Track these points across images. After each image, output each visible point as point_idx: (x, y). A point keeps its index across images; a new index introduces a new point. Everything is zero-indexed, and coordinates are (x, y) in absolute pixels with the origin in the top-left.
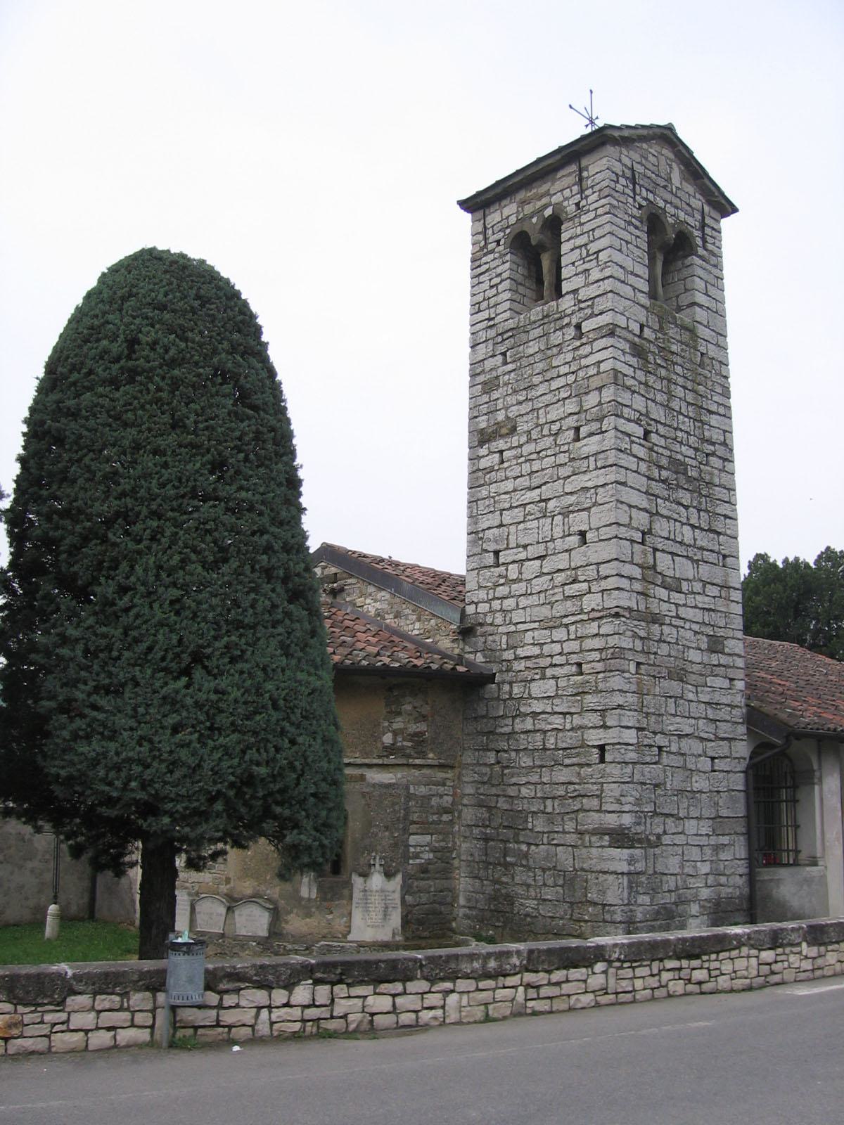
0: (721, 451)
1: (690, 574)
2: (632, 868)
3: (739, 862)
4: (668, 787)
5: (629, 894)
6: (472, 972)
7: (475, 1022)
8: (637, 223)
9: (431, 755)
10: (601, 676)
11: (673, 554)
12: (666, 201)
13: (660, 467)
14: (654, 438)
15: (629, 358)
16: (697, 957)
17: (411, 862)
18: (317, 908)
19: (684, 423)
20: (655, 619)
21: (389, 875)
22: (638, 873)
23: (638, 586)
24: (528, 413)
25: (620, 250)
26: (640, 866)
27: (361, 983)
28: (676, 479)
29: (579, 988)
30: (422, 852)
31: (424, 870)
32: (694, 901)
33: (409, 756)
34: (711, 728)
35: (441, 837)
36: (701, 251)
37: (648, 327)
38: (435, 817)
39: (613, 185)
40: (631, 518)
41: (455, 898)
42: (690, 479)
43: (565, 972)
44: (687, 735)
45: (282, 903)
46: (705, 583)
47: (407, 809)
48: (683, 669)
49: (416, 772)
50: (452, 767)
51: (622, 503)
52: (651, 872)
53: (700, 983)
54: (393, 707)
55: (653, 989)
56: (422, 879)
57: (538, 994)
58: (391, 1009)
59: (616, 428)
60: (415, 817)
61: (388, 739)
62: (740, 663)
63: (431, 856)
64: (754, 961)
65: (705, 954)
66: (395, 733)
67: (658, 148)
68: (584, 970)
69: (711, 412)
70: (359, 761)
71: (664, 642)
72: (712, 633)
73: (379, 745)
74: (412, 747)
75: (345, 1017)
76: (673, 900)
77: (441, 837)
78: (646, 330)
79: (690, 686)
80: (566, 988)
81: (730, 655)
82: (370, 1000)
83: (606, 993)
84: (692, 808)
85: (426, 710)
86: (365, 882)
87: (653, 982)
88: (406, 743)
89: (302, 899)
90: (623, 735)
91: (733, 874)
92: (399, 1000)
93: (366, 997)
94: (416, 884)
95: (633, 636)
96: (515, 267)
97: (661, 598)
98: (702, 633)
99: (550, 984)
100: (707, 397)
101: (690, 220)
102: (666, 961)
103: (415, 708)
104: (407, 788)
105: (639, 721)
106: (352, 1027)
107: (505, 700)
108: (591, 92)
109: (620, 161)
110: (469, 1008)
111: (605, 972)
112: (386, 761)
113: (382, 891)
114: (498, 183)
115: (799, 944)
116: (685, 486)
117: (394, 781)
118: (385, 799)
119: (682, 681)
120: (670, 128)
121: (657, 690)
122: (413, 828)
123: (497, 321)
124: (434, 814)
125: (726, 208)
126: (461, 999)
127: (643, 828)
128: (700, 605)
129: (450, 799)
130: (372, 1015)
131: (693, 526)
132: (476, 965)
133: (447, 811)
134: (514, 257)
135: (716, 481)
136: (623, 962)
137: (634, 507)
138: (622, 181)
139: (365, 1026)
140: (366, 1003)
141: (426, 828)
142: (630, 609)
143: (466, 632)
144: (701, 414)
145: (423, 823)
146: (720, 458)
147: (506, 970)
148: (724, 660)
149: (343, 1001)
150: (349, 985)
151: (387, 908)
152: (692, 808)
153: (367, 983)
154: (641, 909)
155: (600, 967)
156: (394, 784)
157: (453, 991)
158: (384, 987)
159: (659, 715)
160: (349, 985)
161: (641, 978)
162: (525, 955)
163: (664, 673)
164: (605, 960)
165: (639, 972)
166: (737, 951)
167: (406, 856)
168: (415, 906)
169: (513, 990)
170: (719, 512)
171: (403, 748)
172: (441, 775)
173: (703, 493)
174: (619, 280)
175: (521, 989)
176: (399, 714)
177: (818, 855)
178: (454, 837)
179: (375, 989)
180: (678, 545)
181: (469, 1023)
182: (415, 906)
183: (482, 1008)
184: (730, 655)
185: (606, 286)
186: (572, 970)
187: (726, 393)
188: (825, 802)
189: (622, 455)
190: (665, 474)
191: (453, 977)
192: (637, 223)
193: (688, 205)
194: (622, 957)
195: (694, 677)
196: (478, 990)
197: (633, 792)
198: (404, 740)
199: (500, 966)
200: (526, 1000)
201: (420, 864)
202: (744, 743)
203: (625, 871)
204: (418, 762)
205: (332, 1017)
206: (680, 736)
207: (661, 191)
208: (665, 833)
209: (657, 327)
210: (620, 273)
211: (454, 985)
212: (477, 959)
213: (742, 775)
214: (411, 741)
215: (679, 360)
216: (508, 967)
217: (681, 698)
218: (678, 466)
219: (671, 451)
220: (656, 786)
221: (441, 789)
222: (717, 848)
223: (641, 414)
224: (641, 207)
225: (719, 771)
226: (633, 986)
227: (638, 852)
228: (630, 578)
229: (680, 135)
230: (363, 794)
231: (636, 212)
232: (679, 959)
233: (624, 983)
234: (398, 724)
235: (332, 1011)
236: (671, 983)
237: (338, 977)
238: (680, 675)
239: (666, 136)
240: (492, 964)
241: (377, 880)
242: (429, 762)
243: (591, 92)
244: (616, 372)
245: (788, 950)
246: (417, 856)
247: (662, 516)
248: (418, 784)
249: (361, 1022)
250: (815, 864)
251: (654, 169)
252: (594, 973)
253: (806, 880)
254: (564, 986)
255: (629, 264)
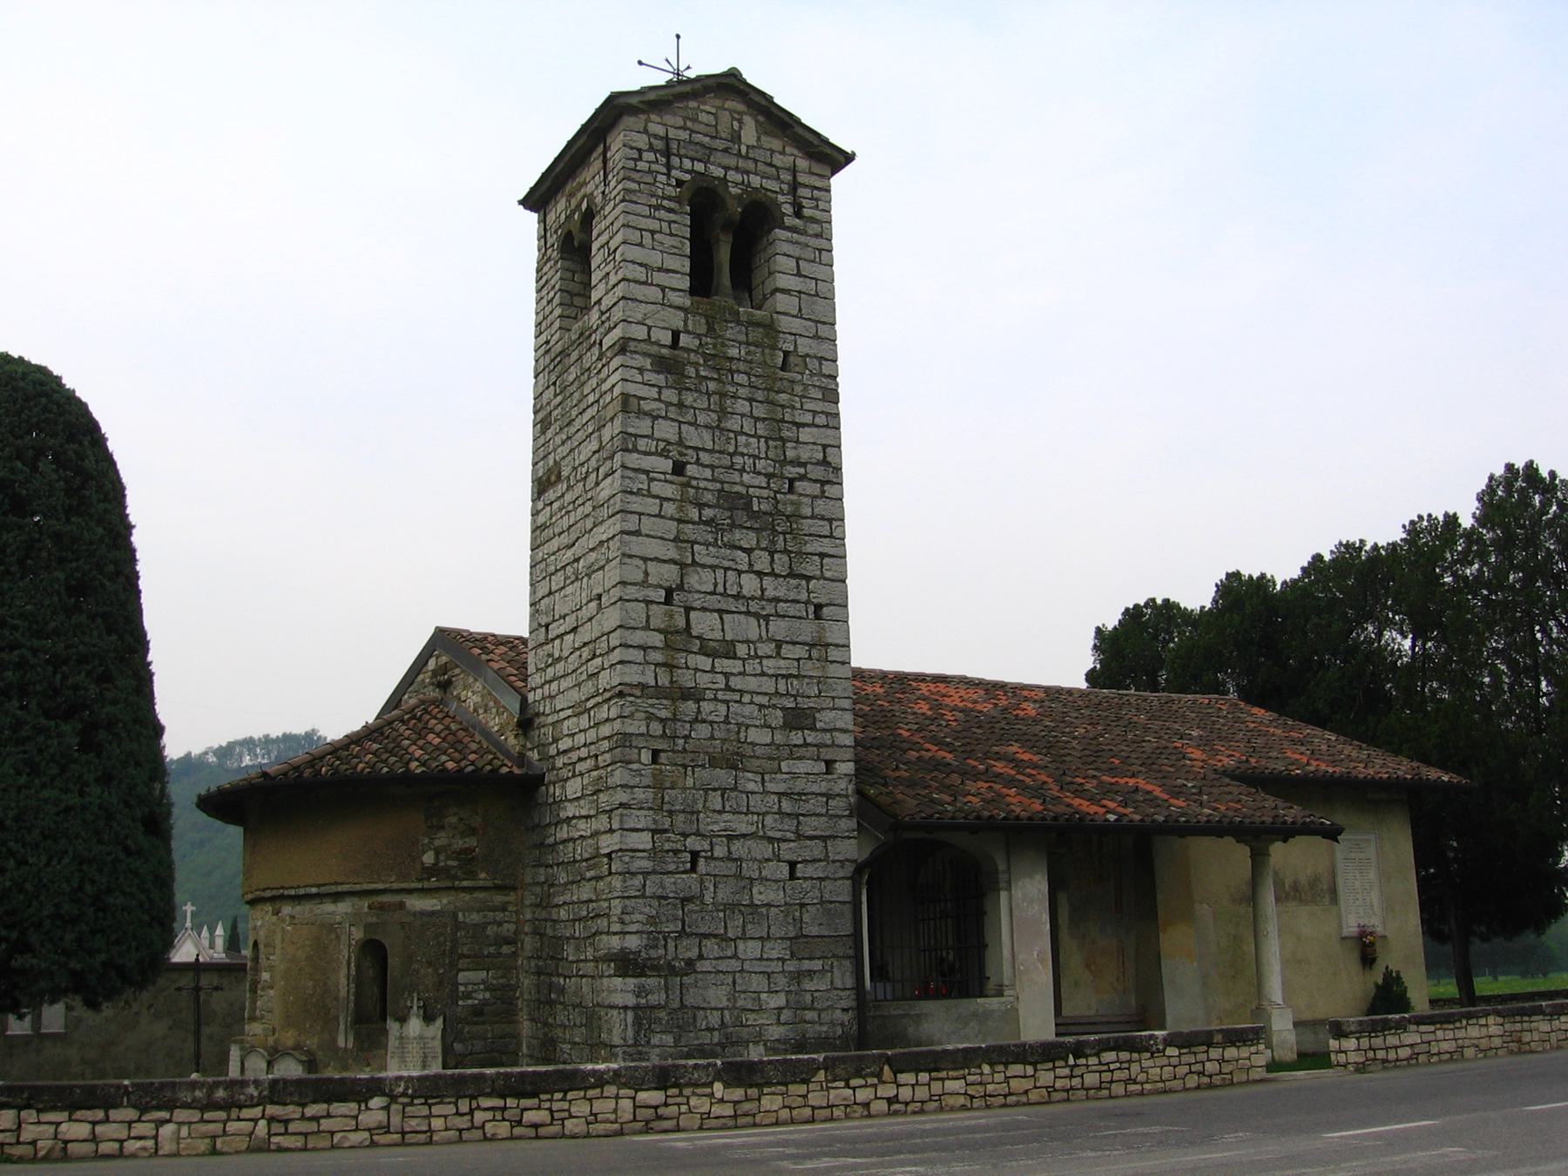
0: (816, 472)
1: (753, 634)
2: (643, 1001)
3: (841, 993)
4: (708, 899)
5: (637, 1033)
6: (193, 1101)
7: (197, 1155)
8: (672, 205)
9: (483, 875)
10: (609, 769)
11: (721, 612)
12: (727, 168)
13: (701, 506)
14: (691, 470)
15: (650, 377)
16: (534, 1095)
17: (460, 1003)
18: (354, 1059)
19: (747, 445)
20: (694, 694)
21: (428, 1019)
22: (653, 1007)
23: (657, 657)
24: (568, 455)
25: (640, 245)
26: (653, 999)
27: (54, 1108)
28: (730, 518)
29: (346, 1126)
30: (476, 991)
31: (478, 1011)
32: (756, 1043)
33: (455, 878)
34: (790, 824)
35: (500, 973)
36: (788, 221)
37: (688, 332)
38: (492, 949)
39: (631, 164)
40: (646, 574)
41: (519, 1045)
42: (754, 515)
43: (325, 1106)
44: (744, 836)
45: (320, 1055)
46: (779, 644)
47: (455, 941)
48: (737, 754)
49: (467, 897)
50: (514, 889)
51: (630, 556)
52: (676, 1004)
53: (536, 1126)
54: (434, 820)
55: (460, 1131)
56: (476, 1023)
57: (286, 1129)
58: (91, 1137)
59: (623, 466)
60: (465, 950)
61: (428, 858)
62: (847, 740)
63: (487, 995)
64: (626, 1104)
65: (546, 1092)
66: (437, 853)
67: (718, 102)
68: (354, 1105)
69: (799, 425)
70: (395, 886)
71: (704, 721)
72: (793, 705)
73: (418, 866)
74: (459, 867)
75: (34, 1143)
76: (716, 1040)
77: (500, 973)
78: (683, 337)
79: (750, 775)
80: (326, 1124)
81: (824, 730)
82: (64, 1127)
83: (388, 1132)
84: (750, 926)
85: (477, 821)
86: (401, 1027)
87: (463, 1122)
88: (450, 863)
89: (338, 1048)
90: (629, 840)
91: (831, 1007)
92: (99, 1129)
93: (61, 1123)
94: (467, 1029)
95: (647, 718)
96: (569, 275)
97: (698, 670)
98: (774, 707)
99: (303, 1118)
100: (793, 408)
101: (772, 185)
102: (480, 1099)
103: (462, 820)
104: (455, 916)
105: (655, 822)
106: (41, 1153)
107: (550, 805)
108: (678, 37)
109: (646, 131)
110: (189, 1140)
111: (387, 1108)
112: (426, 885)
113: (421, 1037)
114: (544, 176)
115: (710, 1084)
116: (748, 524)
117: (439, 908)
118: (428, 929)
119: (736, 768)
120: (733, 74)
121: (690, 782)
122: (462, 963)
123: (552, 343)
124: (491, 945)
125: (837, 159)
126: (179, 1130)
127: (661, 952)
128: (770, 672)
129: (512, 927)
130: (66, 1142)
131: (760, 574)
132: (198, 1093)
133: (508, 942)
134: (568, 264)
135: (807, 511)
136: (413, 1097)
137: (651, 560)
138: (650, 156)
139: (57, 1153)
140: (60, 1129)
141: (478, 962)
142: (643, 686)
143: (526, 723)
144: (778, 430)
145: (475, 956)
146: (816, 481)
147: (240, 1100)
148: (811, 737)
149: (31, 1127)
150: (39, 1111)
151: (425, 1057)
152: (750, 926)
153: (62, 1109)
154: (657, 1050)
155: (376, 1102)
156: (439, 911)
157: (169, 1121)
158: (79, 1114)
159: (692, 813)
160: (39, 1111)
161: (442, 1117)
162: (266, 1085)
163: (703, 759)
164: (384, 1094)
165: (436, 1110)
166: (599, 1090)
167: (454, 997)
168: (466, 1056)
169: (252, 1123)
170: (809, 550)
171: (447, 869)
172: (499, 899)
173: (779, 529)
174: (636, 282)
175: (262, 1123)
176: (442, 828)
177: (1006, 982)
178: (518, 974)
179: (70, 1116)
180: (731, 600)
181: (189, 1155)
182: (466, 1056)
183: (207, 1141)
184: (824, 730)
185: (619, 292)
186: (336, 1105)
187: (832, 396)
188: (1015, 913)
189: (633, 498)
190: (708, 513)
191: (171, 1106)
192: (672, 205)
193: (771, 165)
194: (410, 1091)
195: (757, 762)
196: (202, 1120)
197: (644, 910)
198: (448, 858)
199: (232, 1097)
200: (270, 1135)
201: (472, 1006)
202: (852, 841)
203: (630, 1004)
204: (465, 883)
205: (18, 1143)
206: (730, 838)
207: (719, 157)
208: (701, 957)
209: (703, 330)
210: (640, 273)
211: (171, 1115)
212: (200, 1089)
213: (848, 882)
214: (457, 859)
215: (742, 366)
216: (242, 1097)
217: (735, 789)
218: (736, 502)
219: (722, 483)
220: (685, 900)
221: (499, 916)
222: (798, 976)
223: (669, 443)
224: (680, 183)
225: (805, 879)
226: (430, 1125)
227: (651, 982)
228: (644, 648)
229: (749, 81)
230: (403, 925)
231: (671, 191)
232: (504, 1097)
233: (414, 1122)
234: (441, 839)
235: (18, 1137)
236: (488, 1126)
237: (25, 1102)
238: (733, 761)
239: (730, 85)
240: (220, 1094)
241: (415, 1026)
242: (481, 883)
243: (678, 37)
244: (625, 397)
245: (687, 1091)
246: (468, 996)
247: (703, 566)
248: (470, 910)
249: (51, 1150)
250: (1000, 994)
251: (712, 131)
252: (368, 1108)
253: (975, 1015)
254: (322, 1121)
255: (655, 259)
